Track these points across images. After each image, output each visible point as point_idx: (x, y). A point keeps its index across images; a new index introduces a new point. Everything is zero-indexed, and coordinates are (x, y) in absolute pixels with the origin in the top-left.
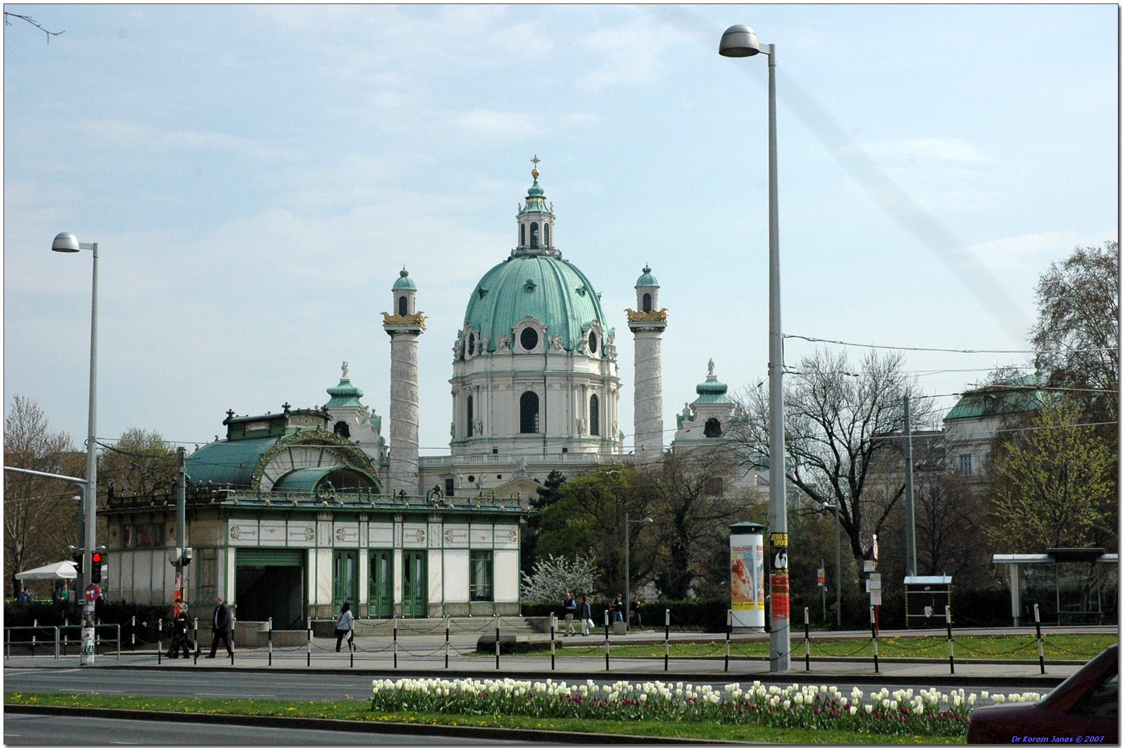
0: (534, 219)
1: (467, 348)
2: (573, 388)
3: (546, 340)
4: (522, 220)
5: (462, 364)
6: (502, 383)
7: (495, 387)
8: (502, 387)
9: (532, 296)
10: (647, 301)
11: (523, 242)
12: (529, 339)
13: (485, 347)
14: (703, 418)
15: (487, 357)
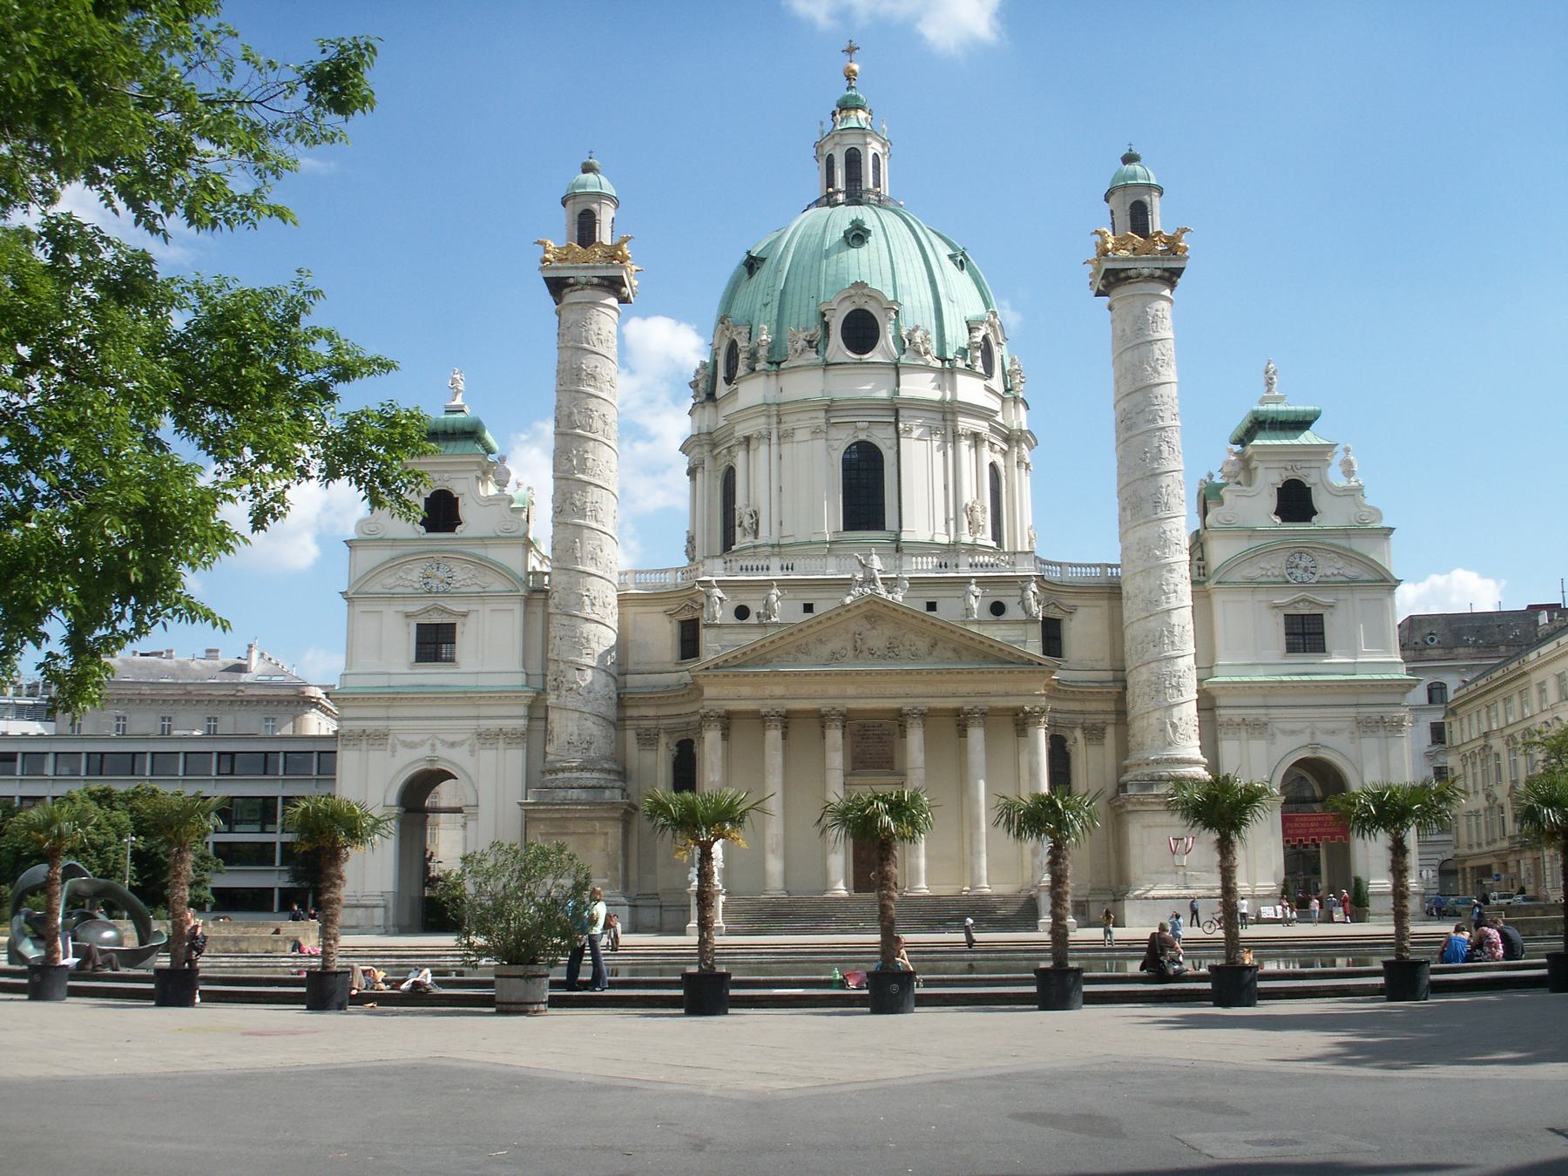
0: (852, 141)
1: (721, 373)
2: (956, 436)
3: (899, 339)
4: (827, 150)
5: (709, 409)
6: (802, 425)
7: (784, 437)
8: (802, 435)
9: (863, 252)
10: (1139, 216)
11: (830, 182)
12: (861, 331)
13: (762, 352)
14: (1269, 481)
15: (767, 373)
